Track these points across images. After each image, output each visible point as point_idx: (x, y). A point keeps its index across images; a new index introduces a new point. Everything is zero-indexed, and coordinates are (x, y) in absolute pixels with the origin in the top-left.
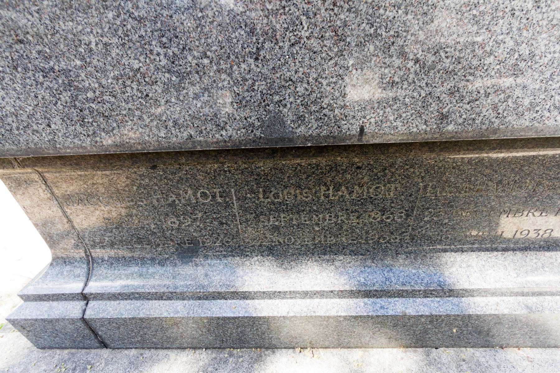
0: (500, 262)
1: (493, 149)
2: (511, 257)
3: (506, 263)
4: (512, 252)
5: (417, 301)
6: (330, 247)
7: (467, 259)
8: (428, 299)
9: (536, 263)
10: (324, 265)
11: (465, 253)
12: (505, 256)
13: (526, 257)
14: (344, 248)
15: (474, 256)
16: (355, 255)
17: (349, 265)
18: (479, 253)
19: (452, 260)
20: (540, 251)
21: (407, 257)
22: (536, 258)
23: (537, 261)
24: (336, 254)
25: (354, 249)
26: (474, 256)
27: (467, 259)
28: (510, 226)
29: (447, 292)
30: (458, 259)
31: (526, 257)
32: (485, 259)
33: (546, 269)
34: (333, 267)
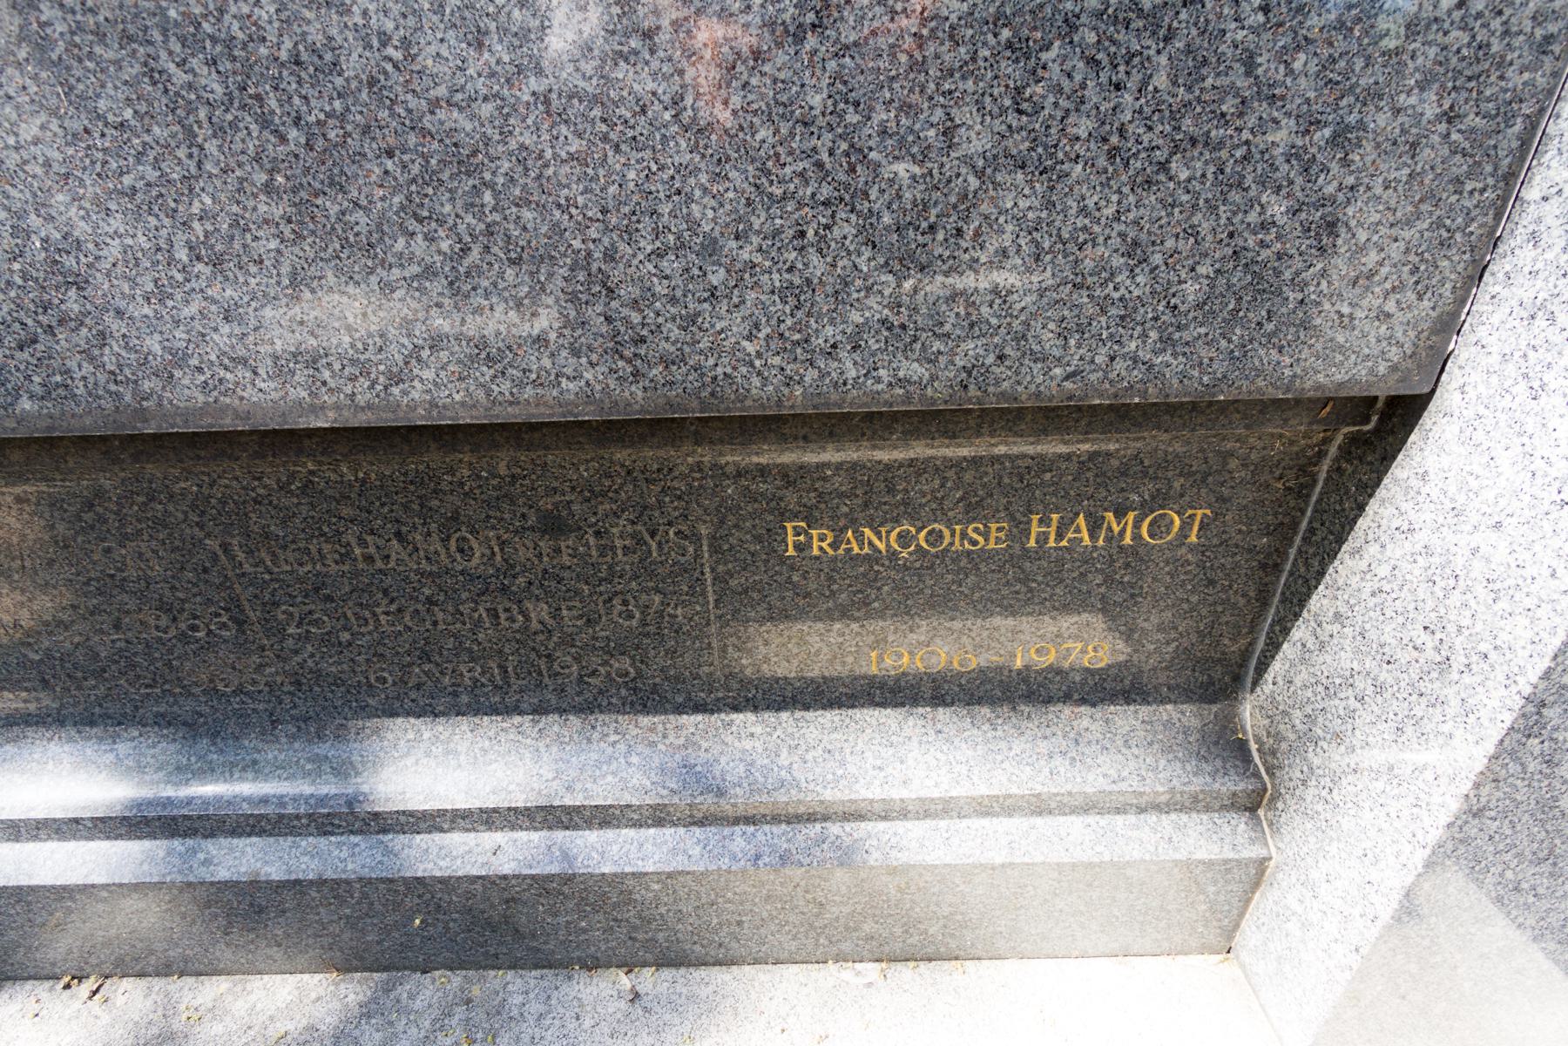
0: (529, 741)
1: (783, 440)
2: (556, 728)
3: (541, 744)
4: (556, 717)
5: (304, 843)
6: (100, 705)
7: (447, 734)
8: (333, 839)
9: (614, 744)
10: (89, 752)
11: (442, 720)
12: (541, 725)
13: (593, 728)
14: (136, 708)
15: (465, 727)
16: (169, 724)
17: (152, 751)
18: (477, 720)
19: (411, 735)
20: (624, 713)
21: (299, 728)
22: (616, 732)
23: (616, 737)
24: (119, 724)
25: (162, 710)
26: (465, 727)
27: (447, 734)
28: (787, 649)
29: (355, 820)
30: (427, 735)
31: (593, 728)
32: (491, 734)
33: (634, 759)
34: (111, 757)
